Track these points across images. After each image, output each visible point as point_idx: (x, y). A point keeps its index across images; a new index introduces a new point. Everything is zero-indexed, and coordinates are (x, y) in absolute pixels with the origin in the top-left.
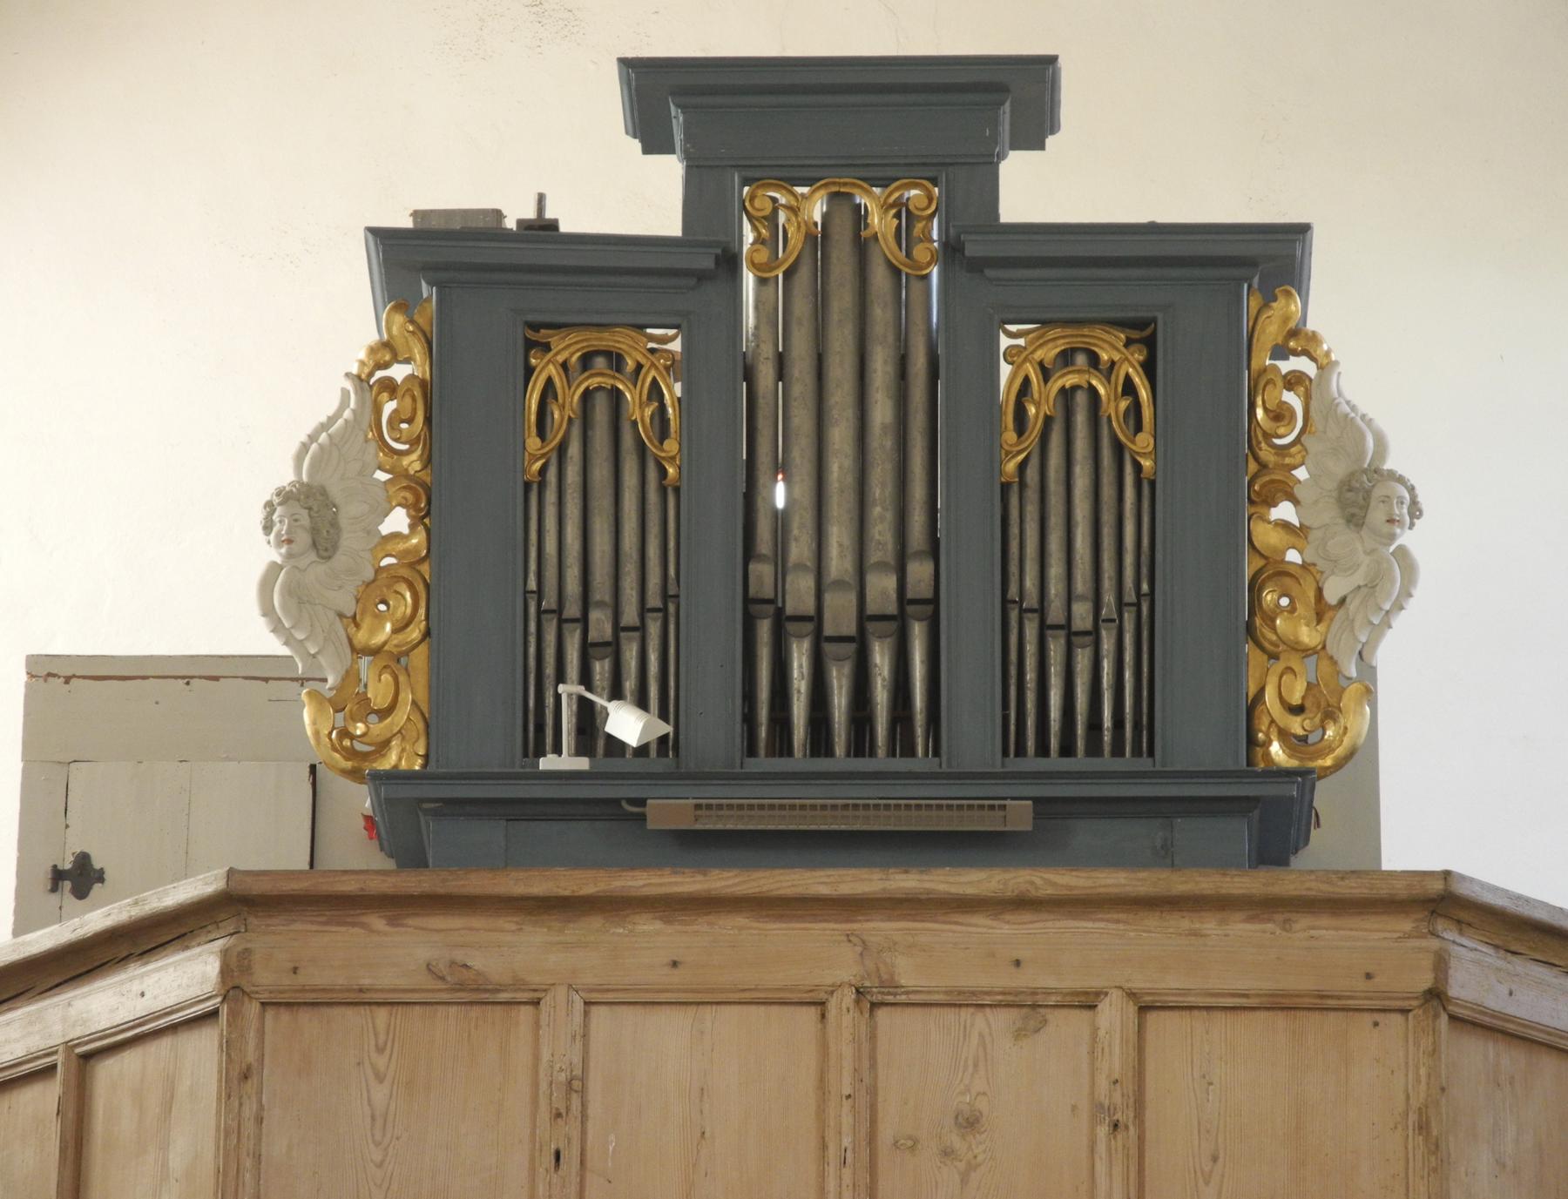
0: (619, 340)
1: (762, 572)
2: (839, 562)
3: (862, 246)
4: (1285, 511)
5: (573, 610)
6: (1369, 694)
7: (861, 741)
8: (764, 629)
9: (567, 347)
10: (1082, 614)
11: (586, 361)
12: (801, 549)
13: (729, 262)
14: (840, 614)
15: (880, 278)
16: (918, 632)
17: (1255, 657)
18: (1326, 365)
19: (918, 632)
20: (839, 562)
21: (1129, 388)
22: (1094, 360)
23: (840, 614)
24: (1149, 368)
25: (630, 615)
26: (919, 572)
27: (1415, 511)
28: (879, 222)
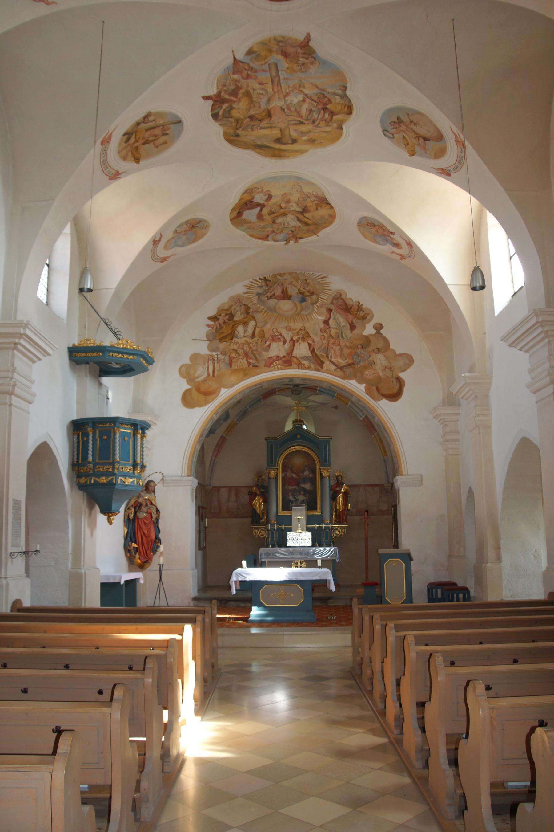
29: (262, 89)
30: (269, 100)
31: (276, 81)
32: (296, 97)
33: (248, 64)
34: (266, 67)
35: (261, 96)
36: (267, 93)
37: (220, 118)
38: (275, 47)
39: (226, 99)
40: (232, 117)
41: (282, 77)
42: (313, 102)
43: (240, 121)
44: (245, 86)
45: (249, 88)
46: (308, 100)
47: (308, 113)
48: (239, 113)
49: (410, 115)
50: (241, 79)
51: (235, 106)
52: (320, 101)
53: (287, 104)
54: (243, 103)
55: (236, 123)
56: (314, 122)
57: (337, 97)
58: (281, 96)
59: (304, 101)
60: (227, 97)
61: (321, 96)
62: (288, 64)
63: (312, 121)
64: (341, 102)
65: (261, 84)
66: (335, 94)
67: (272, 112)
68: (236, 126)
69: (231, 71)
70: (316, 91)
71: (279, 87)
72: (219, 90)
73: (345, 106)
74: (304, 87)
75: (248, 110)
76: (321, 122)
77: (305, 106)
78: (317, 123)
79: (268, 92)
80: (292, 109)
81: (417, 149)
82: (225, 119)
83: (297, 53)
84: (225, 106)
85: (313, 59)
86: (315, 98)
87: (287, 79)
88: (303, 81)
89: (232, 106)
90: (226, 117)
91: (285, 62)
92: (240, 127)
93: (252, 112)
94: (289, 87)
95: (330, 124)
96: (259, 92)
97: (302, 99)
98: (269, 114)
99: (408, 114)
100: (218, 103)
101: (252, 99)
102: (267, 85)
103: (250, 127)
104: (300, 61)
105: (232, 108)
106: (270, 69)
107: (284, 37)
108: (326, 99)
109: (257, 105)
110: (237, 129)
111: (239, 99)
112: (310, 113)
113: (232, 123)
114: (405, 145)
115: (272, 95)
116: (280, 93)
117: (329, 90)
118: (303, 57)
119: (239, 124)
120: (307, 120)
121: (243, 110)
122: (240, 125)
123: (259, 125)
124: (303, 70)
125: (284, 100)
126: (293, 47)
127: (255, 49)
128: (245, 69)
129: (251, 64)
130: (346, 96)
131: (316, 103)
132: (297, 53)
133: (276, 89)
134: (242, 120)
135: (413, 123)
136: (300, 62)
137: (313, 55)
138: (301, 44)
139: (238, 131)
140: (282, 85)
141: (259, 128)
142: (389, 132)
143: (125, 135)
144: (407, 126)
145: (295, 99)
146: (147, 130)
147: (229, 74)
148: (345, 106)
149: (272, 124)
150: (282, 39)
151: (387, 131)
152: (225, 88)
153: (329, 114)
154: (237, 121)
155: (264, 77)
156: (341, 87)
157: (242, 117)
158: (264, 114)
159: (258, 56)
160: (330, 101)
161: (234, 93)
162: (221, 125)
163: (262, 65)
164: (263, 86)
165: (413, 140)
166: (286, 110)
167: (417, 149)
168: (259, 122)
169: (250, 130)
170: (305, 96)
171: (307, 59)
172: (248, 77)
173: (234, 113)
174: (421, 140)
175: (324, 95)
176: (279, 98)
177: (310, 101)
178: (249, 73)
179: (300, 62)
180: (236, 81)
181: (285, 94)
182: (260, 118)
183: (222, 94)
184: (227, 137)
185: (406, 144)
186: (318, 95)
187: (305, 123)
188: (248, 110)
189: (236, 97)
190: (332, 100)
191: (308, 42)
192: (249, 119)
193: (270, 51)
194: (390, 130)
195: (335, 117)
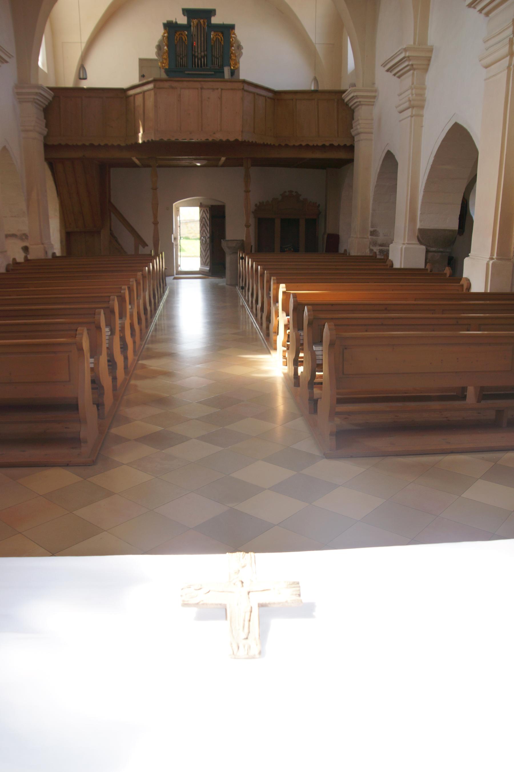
0: (182, 33)
1: (194, 52)
2: (199, 52)
4: (233, 48)
5: (179, 55)
6: (239, 63)
7: (201, 66)
8: (194, 57)
9: (178, 33)
10: (218, 56)
11: (180, 34)
12: (196, 50)
13: (190, 26)
14: (199, 56)
15: (202, 28)
17: (231, 61)
18: (236, 36)
20: (199, 52)
21: (221, 38)
22: (219, 35)
23: (199, 56)
24: (223, 36)
25: (183, 56)
26: (205, 52)
27: (243, 48)
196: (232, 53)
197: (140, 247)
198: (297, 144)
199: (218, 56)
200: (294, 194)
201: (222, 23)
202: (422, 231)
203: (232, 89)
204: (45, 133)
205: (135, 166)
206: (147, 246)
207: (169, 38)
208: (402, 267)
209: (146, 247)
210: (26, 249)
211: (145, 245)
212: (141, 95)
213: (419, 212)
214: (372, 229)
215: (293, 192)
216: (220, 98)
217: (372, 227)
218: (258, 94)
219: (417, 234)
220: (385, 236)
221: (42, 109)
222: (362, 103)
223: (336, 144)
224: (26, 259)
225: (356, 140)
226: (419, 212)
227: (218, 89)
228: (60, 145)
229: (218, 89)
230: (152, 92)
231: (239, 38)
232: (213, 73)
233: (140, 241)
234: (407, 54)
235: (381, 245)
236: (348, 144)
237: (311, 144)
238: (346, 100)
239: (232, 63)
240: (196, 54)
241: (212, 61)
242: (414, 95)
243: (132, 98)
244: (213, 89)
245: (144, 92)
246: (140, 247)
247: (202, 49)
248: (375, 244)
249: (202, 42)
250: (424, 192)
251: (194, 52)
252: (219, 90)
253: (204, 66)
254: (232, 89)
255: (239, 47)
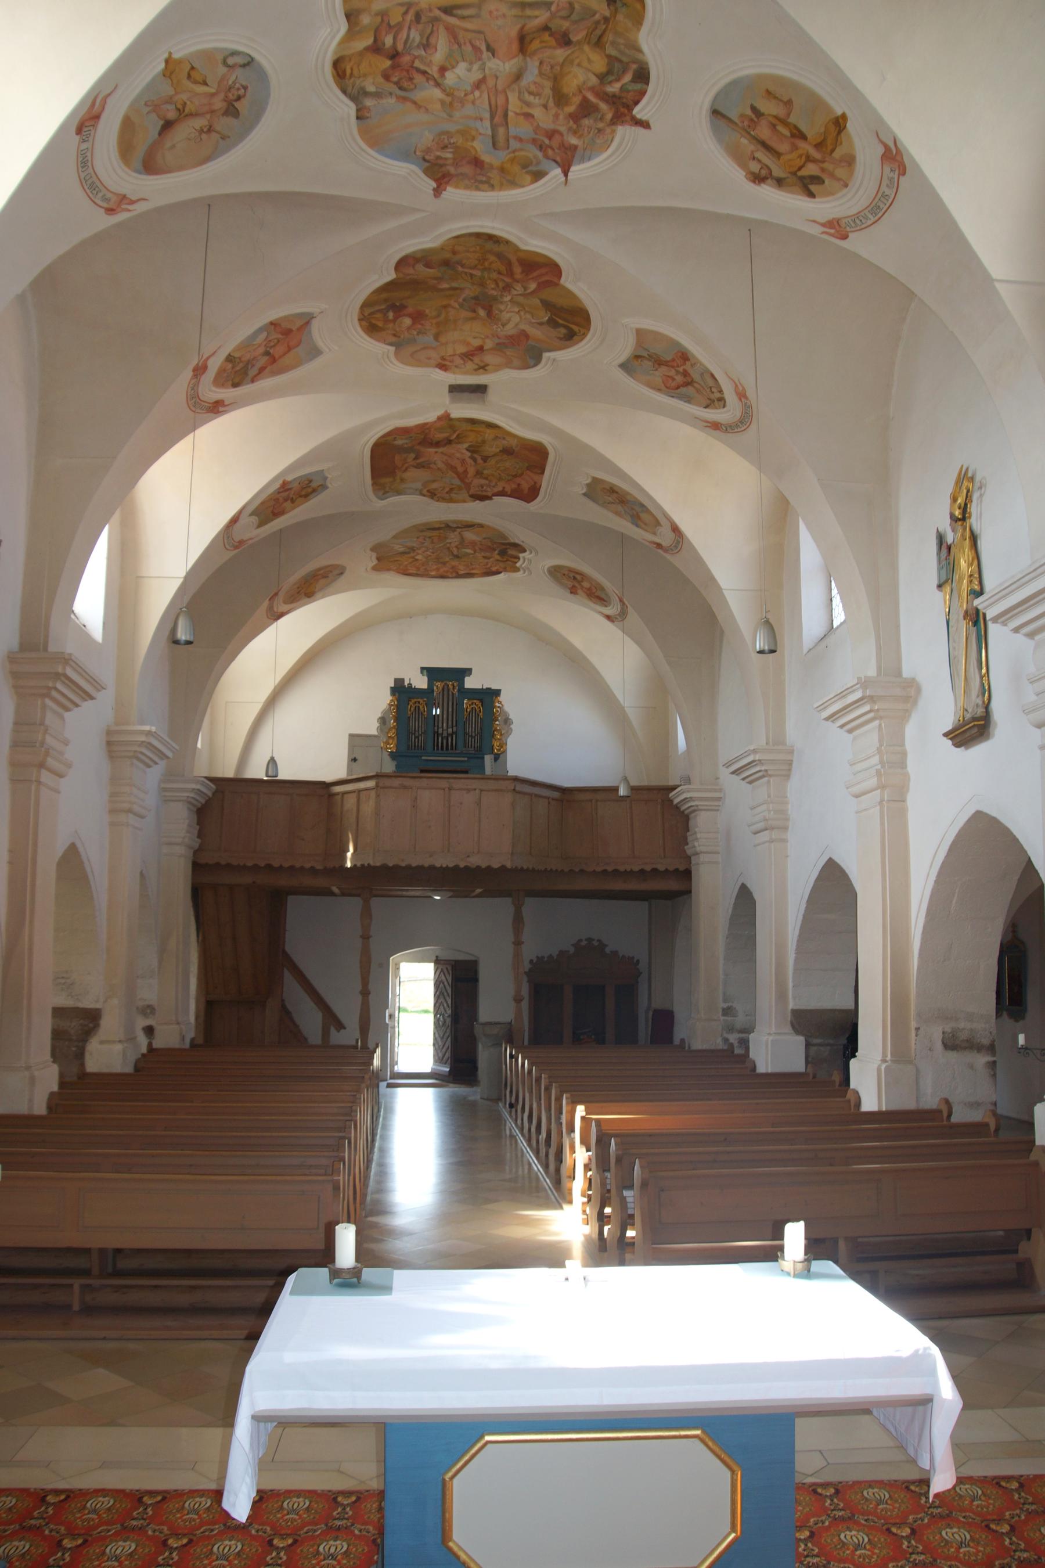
1: (436, 728)
3: (448, 690)
4: (497, 723)
6: (506, 745)
7: (447, 749)
9: (413, 701)
10: (473, 734)
12: (440, 726)
13: (433, 691)
14: (445, 734)
15: (450, 693)
16: (454, 736)
17: (494, 740)
19: (454, 736)
23: (445, 734)
24: (482, 705)
26: (455, 729)
28: (451, 687)
29: (528, 104)
30: (518, 77)
31: (499, 116)
32: (459, 78)
33: (547, 157)
34: (514, 144)
35: (533, 88)
36: (520, 93)
37: (635, 66)
38: (494, 175)
39: (607, 102)
40: (609, 57)
41: (487, 123)
42: (423, 67)
43: (594, 39)
44: (561, 117)
45: (553, 110)
46: (434, 71)
47: (433, 40)
48: (589, 60)
49: (220, 140)
50: (565, 133)
51: (594, 81)
52: (408, 71)
53: (480, 62)
54: (575, 82)
55: (605, 39)
56: (418, 17)
57: (371, 89)
58: (491, 83)
59: (443, 70)
60: (603, 106)
61: (405, 84)
62: (473, 147)
63: (424, 19)
64: (361, 79)
65: (528, 116)
66: (377, 95)
67: (515, 46)
68: (605, 31)
69: (579, 153)
70: (419, 95)
71: (493, 102)
72: (614, 127)
73: (351, 75)
74: (442, 102)
75: (567, 61)
76: (401, 19)
77: (439, 56)
78: (410, 16)
79: (517, 94)
80: (468, 48)
81: (167, 89)
82: (625, 59)
83: (456, 164)
84: (614, 88)
85: (427, 157)
86: (419, 78)
87: (476, 119)
88: (445, 115)
89: (599, 81)
90: (620, 61)
91: (478, 150)
92: (597, 23)
93: (560, 54)
94: (473, 103)
95: (379, 19)
96: (537, 98)
97: (448, 74)
98: (523, 42)
99: (223, 138)
100: (624, 100)
101: (554, 86)
102: (518, 111)
103: (574, 17)
104: (450, 152)
105: (602, 77)
106: (508, 140)
107: (478, 189)
108: (395, 79)
109: (546, 68)
110: (606, 20)
111: (580, 92)
112: (428, 39)
113: (613, 43)
114: (193, 68)
115: (509, 86)
116: (494, 89)
117: (392, 101)
118: (446, 159)
119: (598, 32)
120: (436, 19)
121: (579, 65)
122: (596, 28)
123: (553, 16)
124: (446, 137)
125: (487, 71)
126: (462, 174)
127: (528, 178)
128: (553, 149)
129: (540, 155)
130: (353, 98)
131: (415, 65)
132: (456, 164)
133: (501, 100)
134: (587, 39)
135: (205, 130)
136: (451, 150)
137: (427, 164)
138: (450, 180)
139: (607, 13)
140: (487, 107)
141: (553, 8)
142: (241, 66)
143: (812, 195)
144: (212, 112)
145: (461, 75)
146: (778, 155)
147: (584, 150)
148: (351, 75)
149: (520, 14)
150: (481, 186)
151: (244, 66)
152: (601, 125)
153: (384, 44)
154: (598, 43)
155: (520, 128)
156: (368, 115)
157: (586, 48)
158: (535, 45)
159: (525, 166)
160: (387, 77)
161: (586, 109)
162: (640, 50)
163: (521, 150)
164: (526, 110)
165: (184, 97)
166: (484, 48)
167: (167, 89)
168: (550, 25)
169: (577, 6)
170: (439, 80)
171: (438, 158)
172: (551, 134)
173: (599, 64)
174: (172, 115)
175: (401, 88)
176: (497, 78)
177: (429, 71)
178: (547, 141)
179: (451, 150)
180: (575, 133)
181: (483, 87)
182: (546, 36)
183: (609, 116)
184: (638, 6)
185: (193, 73)
186: (412, 87)
187: (439, 9)
188: (567, 61)
189: (585, 100)
190: (381, 80)
191: (438, 187)
192: (571, 37)
193: (502, 170)
194: (239, 71)
195: (370, 41)
196: (496, 730)
197: (333, 1029)
198: (599, 869)
199: (473, 734)
200: (596, 943)
201: (481, 687)
202: (797, 1014)
203: (496, 790)
204: (196, 846)
205: (333, 894)
206: (345, 1028)
207: (398, 707)
208: (770, 1071)
209: (342, 1031)
210: (149, 1031)
211: (340, 1026)
212: (355, 795)
213: (790, 985)
214: (725, 1005)
215: (594, 940)
216: (479, 803)
217: (725, 1001)
218: (536, 795)
219: (789, 1019)
220: (747, 1015)
221: (195, 810)
222: (700, 807)
223: (661, 868)
224: (151, 1049)
225: (693, 862)
226: (790, 985)
227: (475, 790)
228: (218, 864)
229: (475, 790)
230: (373, 793)
231: (507, 708)
232: (466, 759)
233: (332, 1020)
234: (757, 757)
235: (741, 1031)
236: (682, 868)
237: (622, 869)
238: (676, 802)
239: (496, 744)
240: (440, 731)
241: (465, 741)
242: (772, 812)
243: (339, 797)
244: (469, 790)
245: (360, 791)
246: (333, 1029)
247: (450, 723)
248: (731, 1029)
249: (450, 713)
250: (796, 954)
251: (436, 728)
252: (477, 791)
253: (452, 749)
254: (496, 790)
255: (507, 721)
